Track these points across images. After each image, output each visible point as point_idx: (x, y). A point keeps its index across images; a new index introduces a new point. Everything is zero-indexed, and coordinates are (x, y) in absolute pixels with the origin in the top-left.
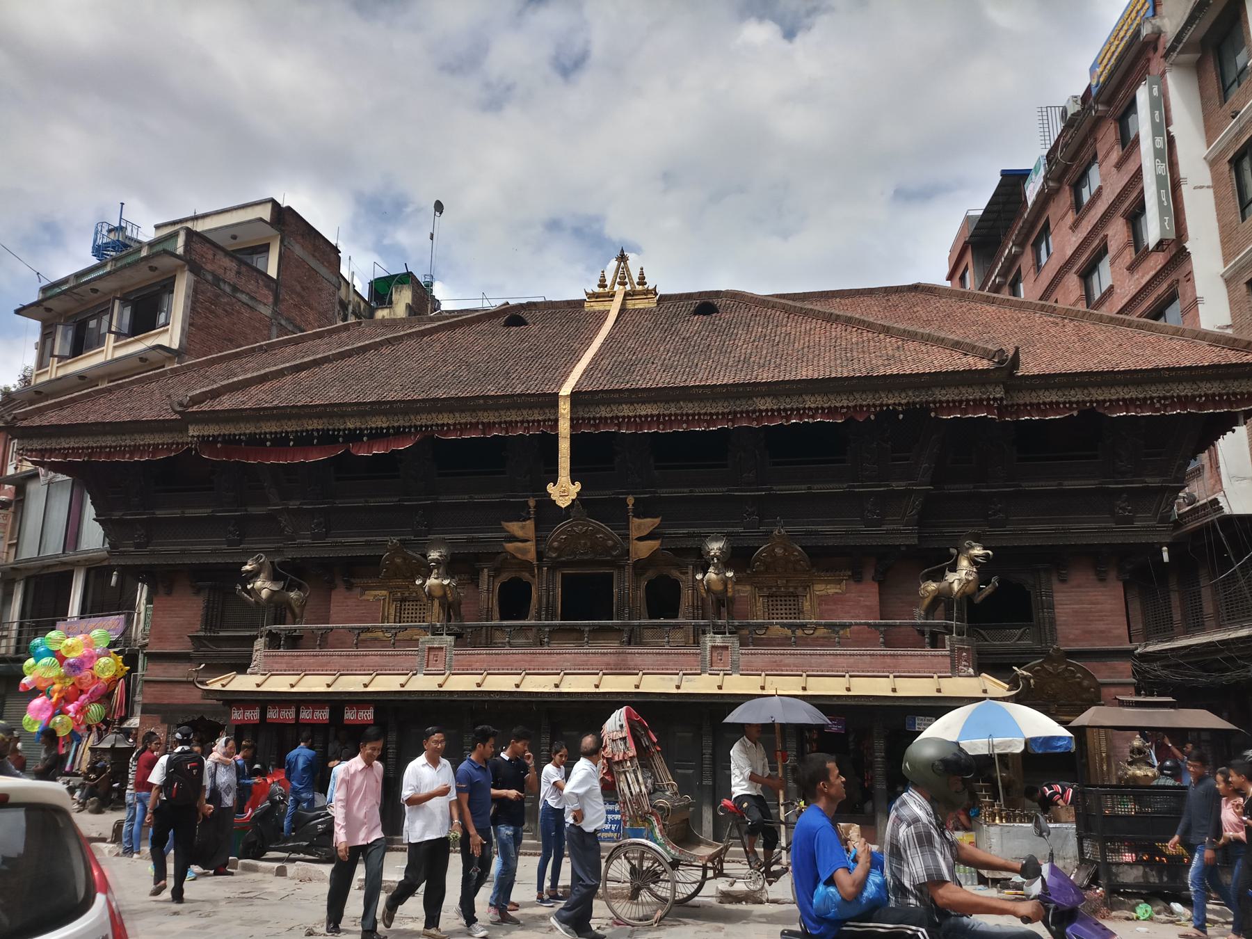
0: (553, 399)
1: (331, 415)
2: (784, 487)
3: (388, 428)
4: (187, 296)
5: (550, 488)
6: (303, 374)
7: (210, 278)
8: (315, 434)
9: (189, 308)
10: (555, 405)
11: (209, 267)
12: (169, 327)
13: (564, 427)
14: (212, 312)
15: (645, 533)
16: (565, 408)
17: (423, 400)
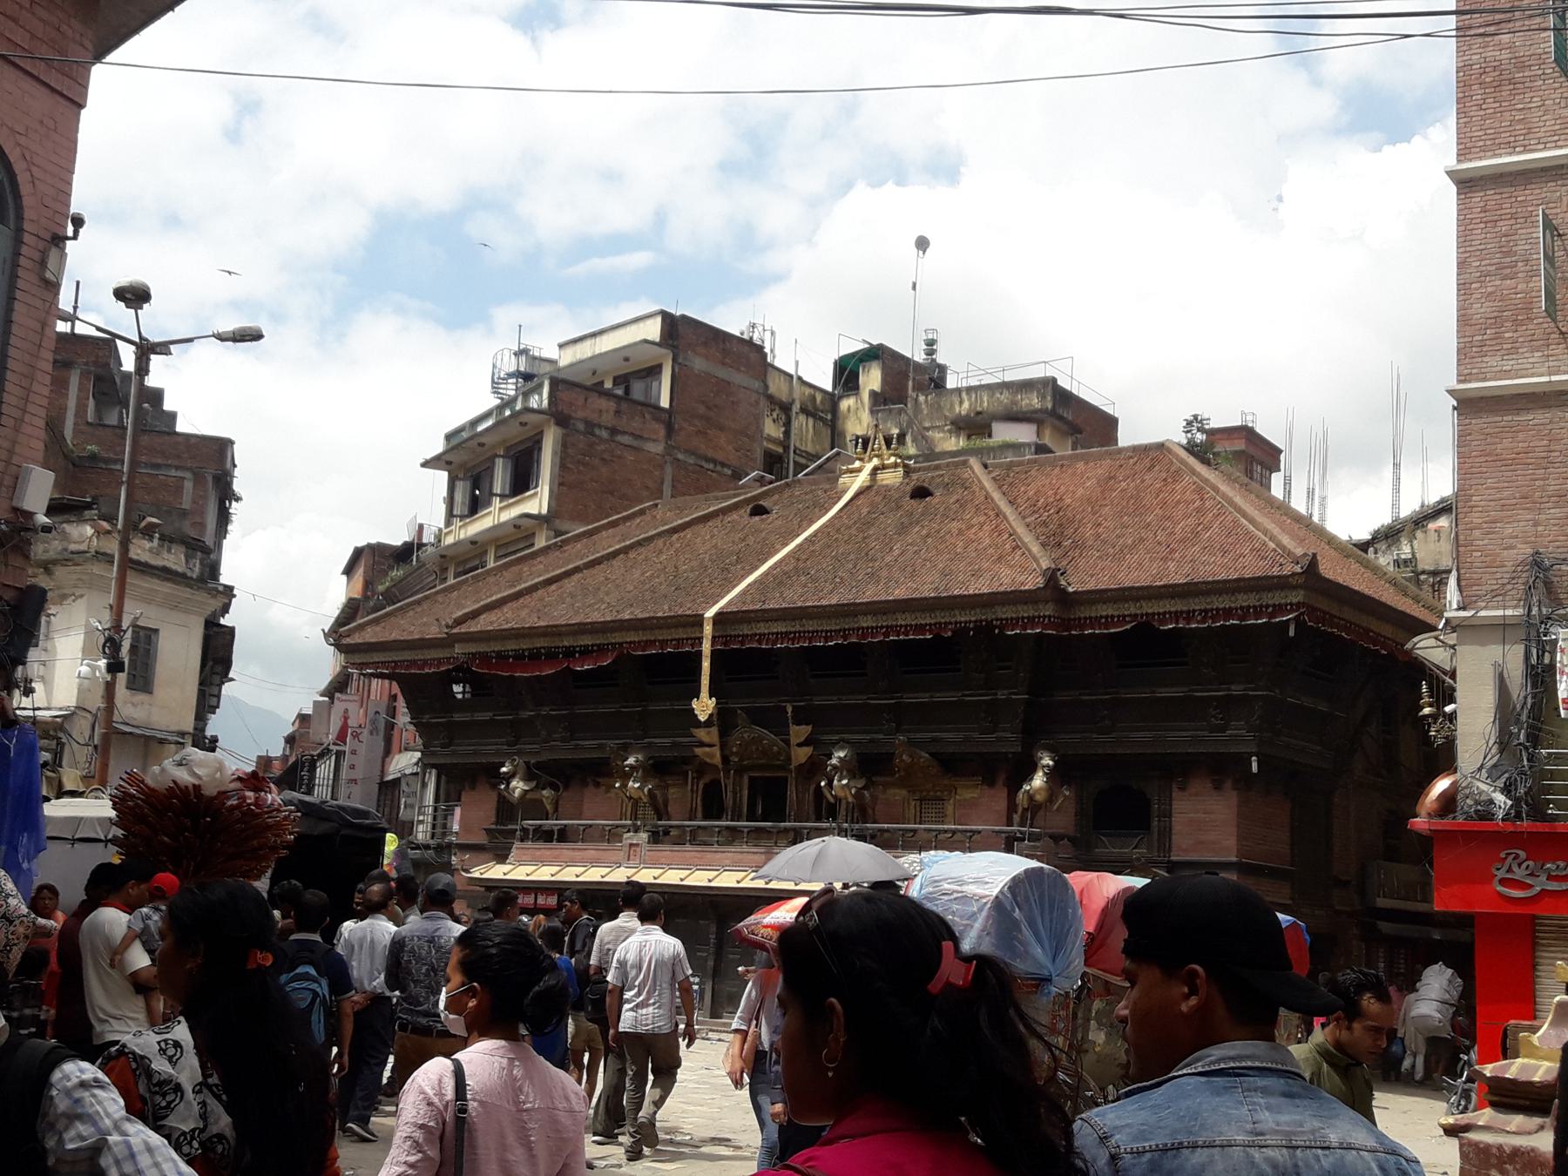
0: (698, 621)
1: (553, 635)
2: (911, 695)
3: (593, 645)
4: (554, 453)
5: (695, 704)
6: (553, 587)
7: (581, 426)
8: (543, 651)
9: (558, 467)
10: (701, 625)
11: (580, 414)
12: (539, 489)
13: (706, 647)
14: (584, 464)
15: (802, 739)
16: (708, 629)
17: (612, 621)
